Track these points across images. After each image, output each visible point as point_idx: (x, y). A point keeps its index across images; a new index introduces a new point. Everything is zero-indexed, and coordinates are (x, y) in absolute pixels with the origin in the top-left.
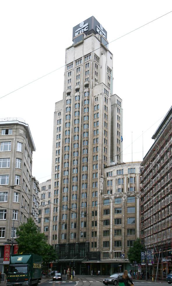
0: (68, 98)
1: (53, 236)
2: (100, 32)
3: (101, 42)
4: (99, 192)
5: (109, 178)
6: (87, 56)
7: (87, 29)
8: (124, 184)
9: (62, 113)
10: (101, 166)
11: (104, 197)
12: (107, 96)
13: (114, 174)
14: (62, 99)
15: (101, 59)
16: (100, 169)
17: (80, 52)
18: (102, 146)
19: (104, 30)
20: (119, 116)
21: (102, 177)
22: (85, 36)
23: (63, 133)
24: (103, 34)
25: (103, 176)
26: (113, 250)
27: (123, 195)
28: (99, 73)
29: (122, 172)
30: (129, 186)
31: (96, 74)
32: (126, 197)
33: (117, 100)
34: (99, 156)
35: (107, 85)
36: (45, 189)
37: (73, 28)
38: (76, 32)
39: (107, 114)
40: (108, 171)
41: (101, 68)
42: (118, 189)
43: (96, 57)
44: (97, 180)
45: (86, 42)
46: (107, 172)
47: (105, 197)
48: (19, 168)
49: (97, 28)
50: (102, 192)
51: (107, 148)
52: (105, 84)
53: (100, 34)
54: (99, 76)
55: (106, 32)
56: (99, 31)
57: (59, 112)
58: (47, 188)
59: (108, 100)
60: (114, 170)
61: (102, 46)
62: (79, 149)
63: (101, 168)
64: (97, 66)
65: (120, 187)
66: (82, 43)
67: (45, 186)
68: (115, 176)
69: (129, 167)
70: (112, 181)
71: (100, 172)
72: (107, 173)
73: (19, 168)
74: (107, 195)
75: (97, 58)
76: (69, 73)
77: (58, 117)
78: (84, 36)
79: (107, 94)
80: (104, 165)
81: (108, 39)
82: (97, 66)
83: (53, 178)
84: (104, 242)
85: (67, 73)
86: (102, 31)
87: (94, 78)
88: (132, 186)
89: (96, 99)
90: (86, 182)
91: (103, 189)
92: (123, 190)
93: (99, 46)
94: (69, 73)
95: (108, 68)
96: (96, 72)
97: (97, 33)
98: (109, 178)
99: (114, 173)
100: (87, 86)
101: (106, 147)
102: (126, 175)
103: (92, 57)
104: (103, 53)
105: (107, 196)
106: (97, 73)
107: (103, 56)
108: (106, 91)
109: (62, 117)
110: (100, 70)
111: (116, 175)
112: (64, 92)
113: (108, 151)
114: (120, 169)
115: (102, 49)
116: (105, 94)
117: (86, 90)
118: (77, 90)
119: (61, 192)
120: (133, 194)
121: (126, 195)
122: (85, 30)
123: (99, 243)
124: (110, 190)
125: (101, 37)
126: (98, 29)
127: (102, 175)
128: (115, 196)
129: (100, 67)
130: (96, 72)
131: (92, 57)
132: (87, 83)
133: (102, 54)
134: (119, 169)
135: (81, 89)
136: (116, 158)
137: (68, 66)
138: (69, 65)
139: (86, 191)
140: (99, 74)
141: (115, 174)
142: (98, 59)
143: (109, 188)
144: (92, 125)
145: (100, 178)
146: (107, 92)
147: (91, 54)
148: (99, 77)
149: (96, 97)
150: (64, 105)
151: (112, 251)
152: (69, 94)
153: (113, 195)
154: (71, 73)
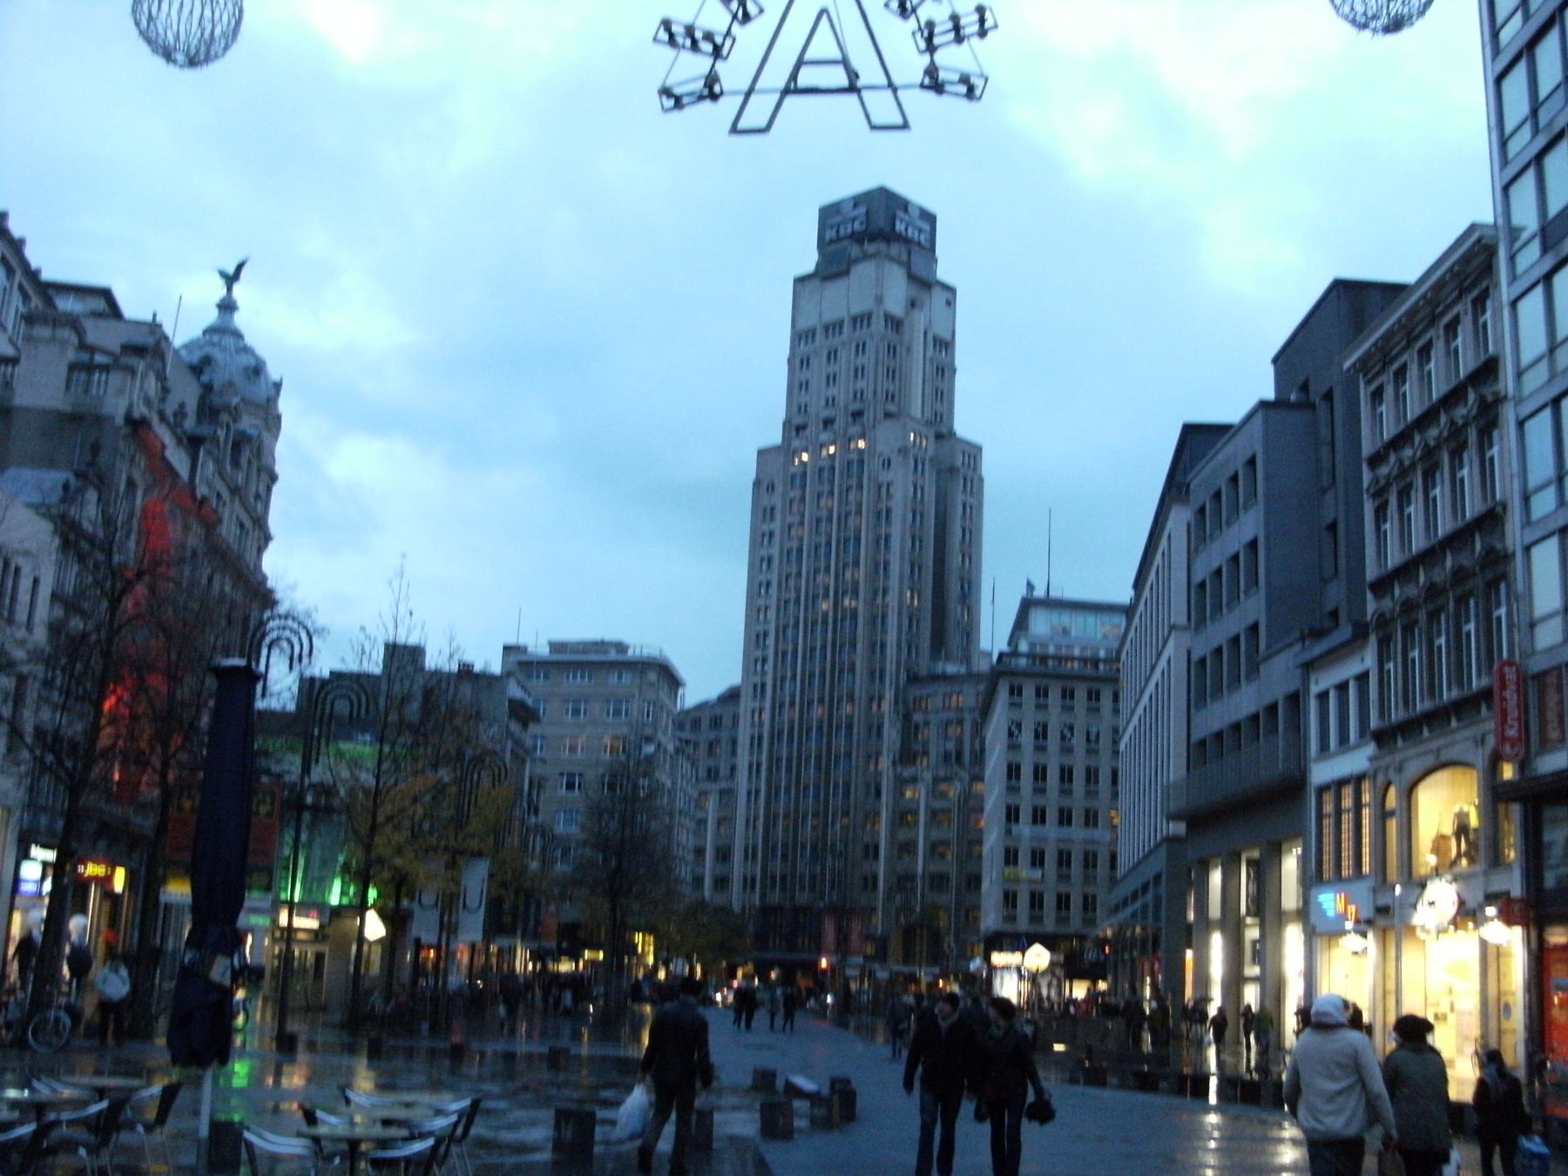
1: (745, 879)
6: (862, 320)
15: (906, 323)
17: (841, 300)
28: (901, 370)
31: (892, 374)
49: (898, 223)
54: (900, 379)
66: (846, 273)
75: (895, 324)
82: (892, 350)
100: (857, 415)
106: (894, 372)
110: (904, 358)
122: (857, 226)
135: (837, 421)
140: (900, 379)
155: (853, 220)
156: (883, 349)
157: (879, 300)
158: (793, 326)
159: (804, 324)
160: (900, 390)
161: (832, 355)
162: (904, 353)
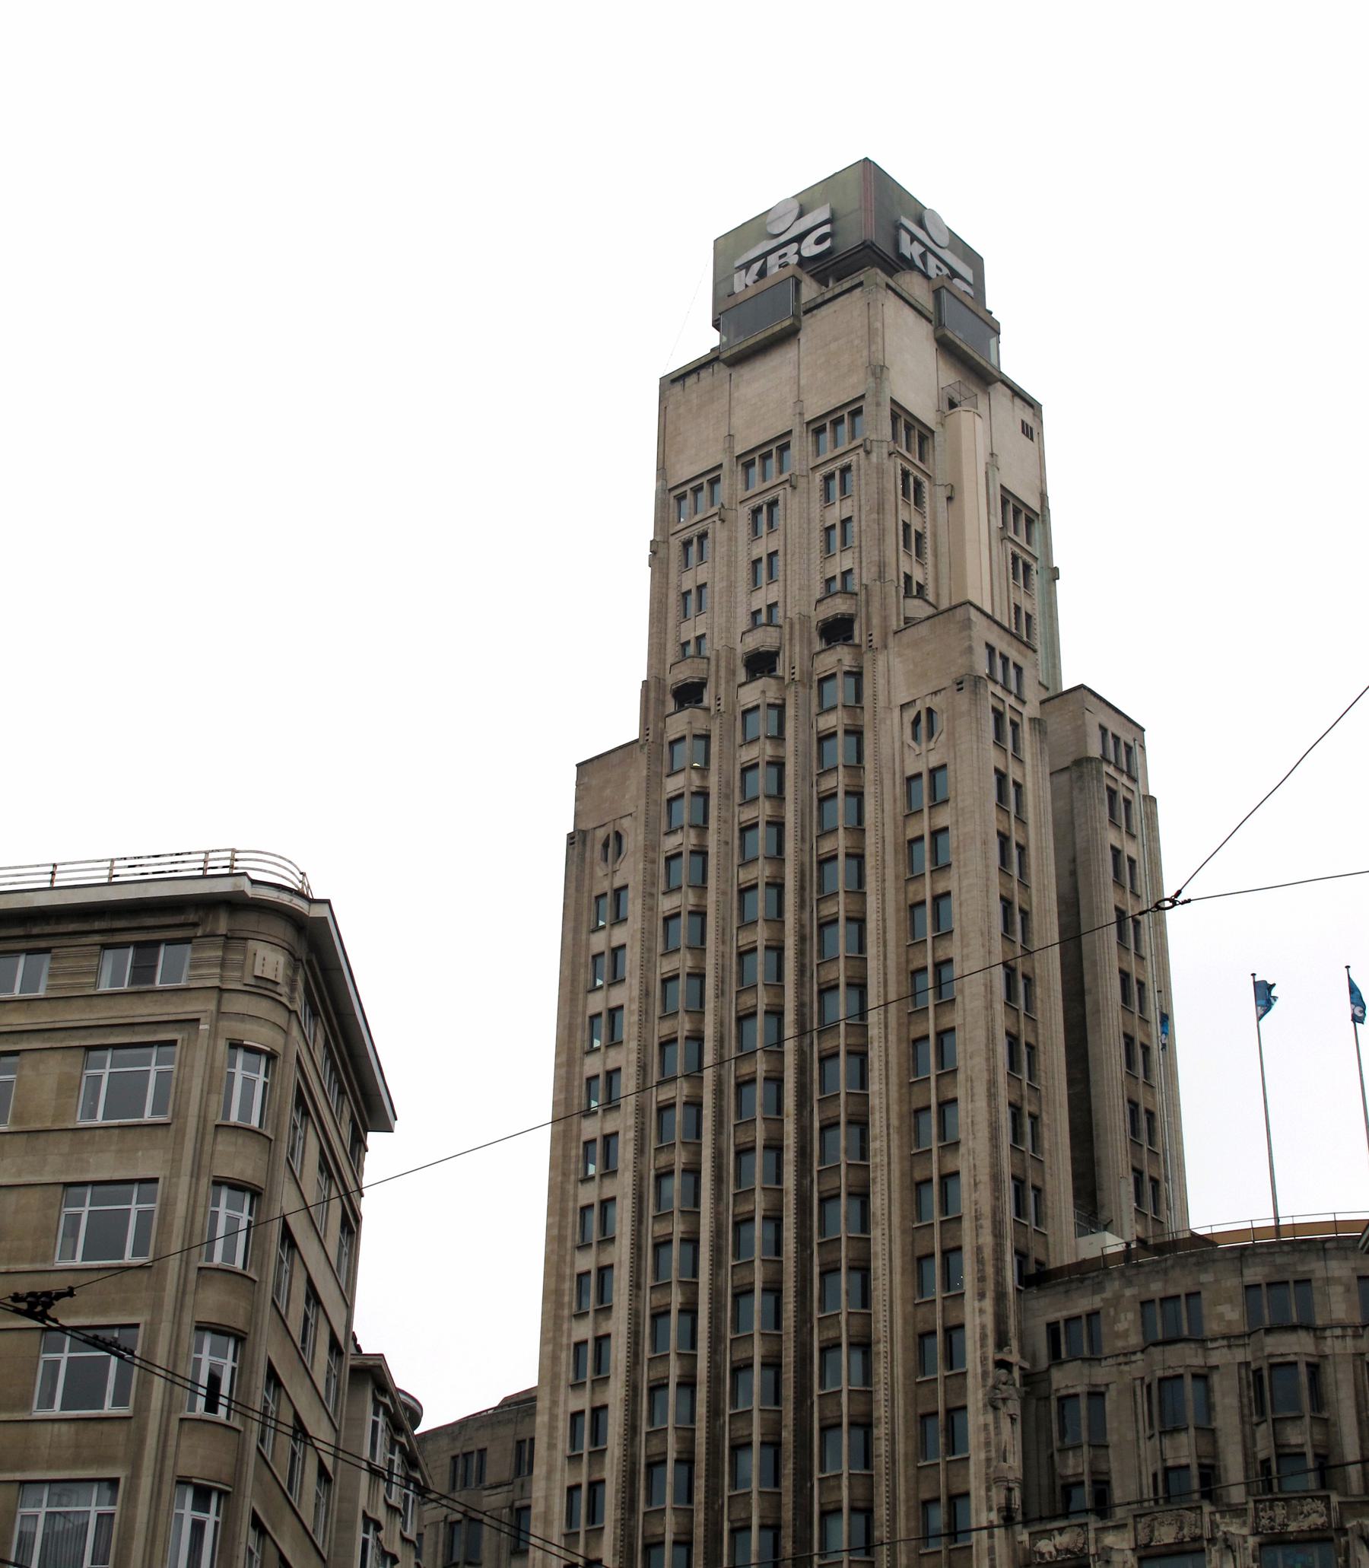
0: (679, 724)
2: (932, 261)
3: (936, 321)
4: (988, 1498)
5: (1067, 1379)
7: (827, 244)
8: (1214, 1425)
9: (635, 839)
10: (990, 1270)
11: (1031, 1552)
12: (1011, 700)
13: (1118, 1335)
14: (629, 730)
16: (981, 1296)
18: (992, 1096)
19: (957, 244)
20: (1130, 849)
21: (1001, 1364)
22: (810, 290)
23: (646, 993)
24: (954, 274)
25: (1014, 1357)
27: (1213, 1523)
28: (935, 535)
29: (1196, 1319)
30: (1264, 1448)
31: (914, 541)
32: (1252, 1541)
33: (1103, 730)
34: (965, 1178)
35: (1005, 618)
36: (481, 1478)
38: (740, 268)
39: (1015, 837)
40: (1058, 1315)
41: (950, 499)
42: (1167, 1470)
43: (909, 428)
44: (963, 1388)
45: (814, 328)
46: (1053, 1316)
47: (1045, 1546)
48: (255, 1123)
49: (905, 238)
50: (1017, 1494)
51: (1034, 1109)
52: (988, 609)
53: (932, 272)
55: (975, 261)
56: (923, 256)
57: (609, 830)
58: (499, 1466)
59: (1026, 728)
60: (1116, 1301)
61: (946, 347)
62: (790, 1127)
63: (990, 1285)
64: (918, 485)
65: (1183, 1450)
66: (789, 335)
67: (482, 1452)
69: (1255, 1274)
70: (1102, 1395)
71: (989, 1320)
72: (1053, 1329)
73: (255, 1123)
74: (1061, 1530)
76: (687, 544)
77: (600, 872)
78: (803, 285)
79: (1013, 687)
80: (1021, 1255)
81: (995, 301)
82: (913, 490)
85: (675, 543)
86: (948, 256)
87: (891, 574)
89: (916, 722)
90: (860, 1408)
91: (1019, 1474)
92: (1210, 1476)
93: (928, 350)
94: (687, 544)
95: (1004, 503)
96: (907, 527)
97: (908, 264)
98: (1067, 1379)
99: (1121, 1327)
100: (836, 631)
101: (1027, 1108)
102: (1231, 1339)
103: (877, 426)
104: (957, 398)
105: (1063, 1540)
106: (920, 536)
107: (964, 417)
108: (999, 662)
109: (630, 871)
111: (1135, 1340)
113: (1046, 1135)
114: (1172, 1291)
115: (949, 376)
116: (991, 687)
117: (839, 658)
118: (761, 664)
119: (629, 1505)
120: (1316, 1520)
121: (1245, 1531)
122: (810, 249)
124: (1086, 1478)
125: (937, 293)
126: (914, 238)
127: (1001, 1342)
128: (1143, 1539)
129: (942, 494)
130: (907, 527)
131: (877, 426)
132: (839, 606)
133: (952, 405)
134: (1156, 1288)
136: (1120, 1194)
137: (681, 498)
138: (687, 488)
139: (860, 1492)
141: (1125, 1326)
142: (922, 439)
143: (1076, 1465)
144: (891, 924)
145: (985, 1374)
146: (1012, 672)
147: (867, 406)
148: (936, 566)
149: (920, 706)
150: (653, 782)
152: (689, 694)
153: (1119, 1527)
154: (707, 543)
155: (800, 238)
156: (893, 483)
157: (878, 371)
158: (662, 470)
159: (685, 470)
160: (937, 580)
161: (765, 513)
162: (942, 502)
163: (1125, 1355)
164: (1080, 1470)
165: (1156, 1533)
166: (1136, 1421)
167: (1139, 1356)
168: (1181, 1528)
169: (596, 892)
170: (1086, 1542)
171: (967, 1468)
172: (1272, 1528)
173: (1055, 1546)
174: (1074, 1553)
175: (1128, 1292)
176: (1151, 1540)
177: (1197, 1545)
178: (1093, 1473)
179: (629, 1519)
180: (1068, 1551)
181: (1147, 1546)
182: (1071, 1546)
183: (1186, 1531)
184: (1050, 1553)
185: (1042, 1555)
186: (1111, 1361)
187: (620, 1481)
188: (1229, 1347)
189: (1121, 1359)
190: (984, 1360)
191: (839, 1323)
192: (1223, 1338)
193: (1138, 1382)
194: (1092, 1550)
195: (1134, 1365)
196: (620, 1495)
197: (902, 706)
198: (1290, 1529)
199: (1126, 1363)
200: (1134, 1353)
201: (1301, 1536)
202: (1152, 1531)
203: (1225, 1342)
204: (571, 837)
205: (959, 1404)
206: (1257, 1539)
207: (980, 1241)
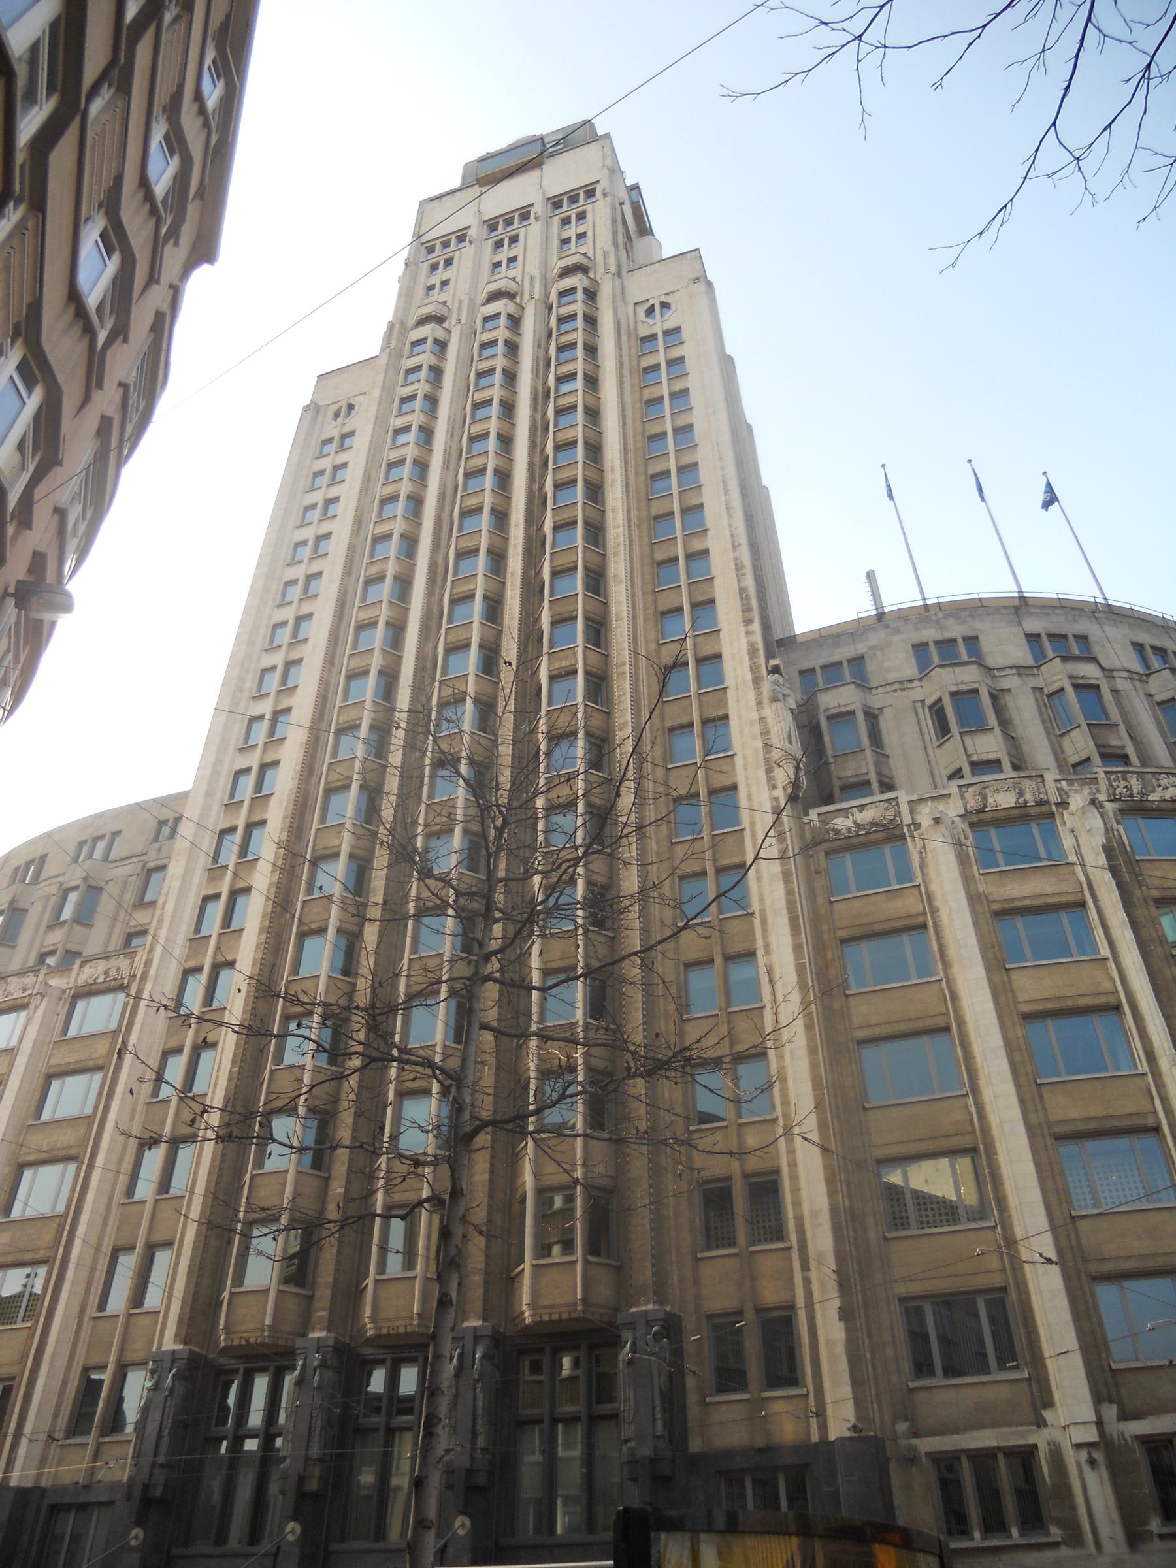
10: (754, 603)
26: (1111, 1412)
37: (467, 167)
63: (756, 615)
68: (903, 684)
74: (861, 808)
83: (209, 794)
84: (912, 1307)
88: (1114, 742)
112: (391, 325)
123: (845, 1314)
128: (973, 803)
151: (1099, 1423)
163: (901, 682)
164: (864, 771)
165: (991, 800)
166: (922, 734)
167: (917, 683)
168: (1021, 794)
169: (324, 437)
170: (898, 813)
171: (733, 765)
172: (1131, 796)
173: (855, 822)
174: (883, 825)
175: (896, 638)
176: (985, 806)
177: (1044, 809)
178: (879, 774)
179: (295, 844)
180: (872, 824)
181: (979, 812)
182: (877, 820)
183: (1028, 796)
184: (849, 829)
185: (837, 832)
186: (881, 690)
187: (291, 808)
188: (1019, 674)
189: (897, 686)
190: (754, 669)
191: (575, 654)
192: (1011, 668)
193: (919, 705)
194: (907, 820)
195: (912, 692)
196: (288, 820)
197: (635, 304)
198: (1150, 798)
199: (902, 689)
200: (911, 681)
201: (1163, 805)
202: (985, 798)
203: (1014, 671)
204: (306, 409)
205: (721, 713)
206: (1115, 805)
207: (742, 585)
